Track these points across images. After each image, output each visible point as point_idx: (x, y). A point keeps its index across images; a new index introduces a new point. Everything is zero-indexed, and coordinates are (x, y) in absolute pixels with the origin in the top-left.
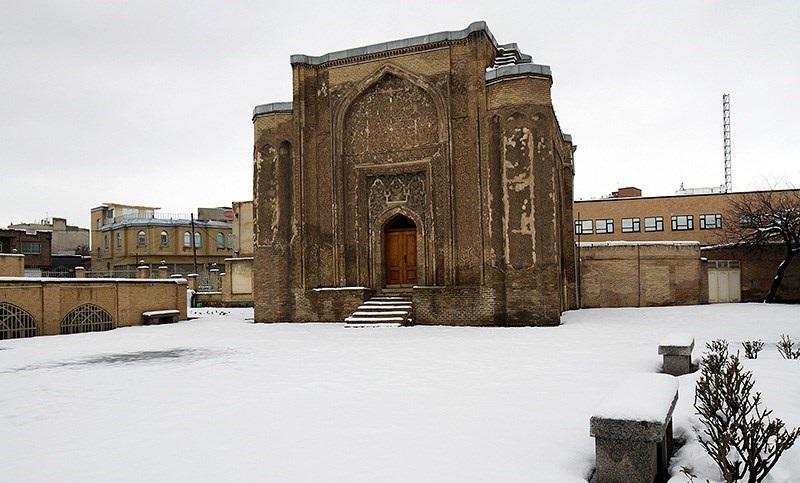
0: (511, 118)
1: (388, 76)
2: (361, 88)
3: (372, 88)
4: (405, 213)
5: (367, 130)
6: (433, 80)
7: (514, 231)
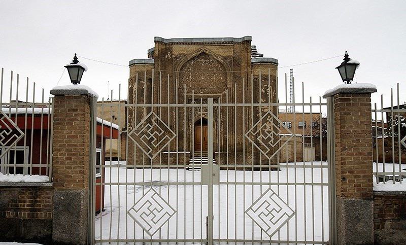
1: (203, 53)
2: (189, 57)
3: (193, 58)
6: (225, 58)
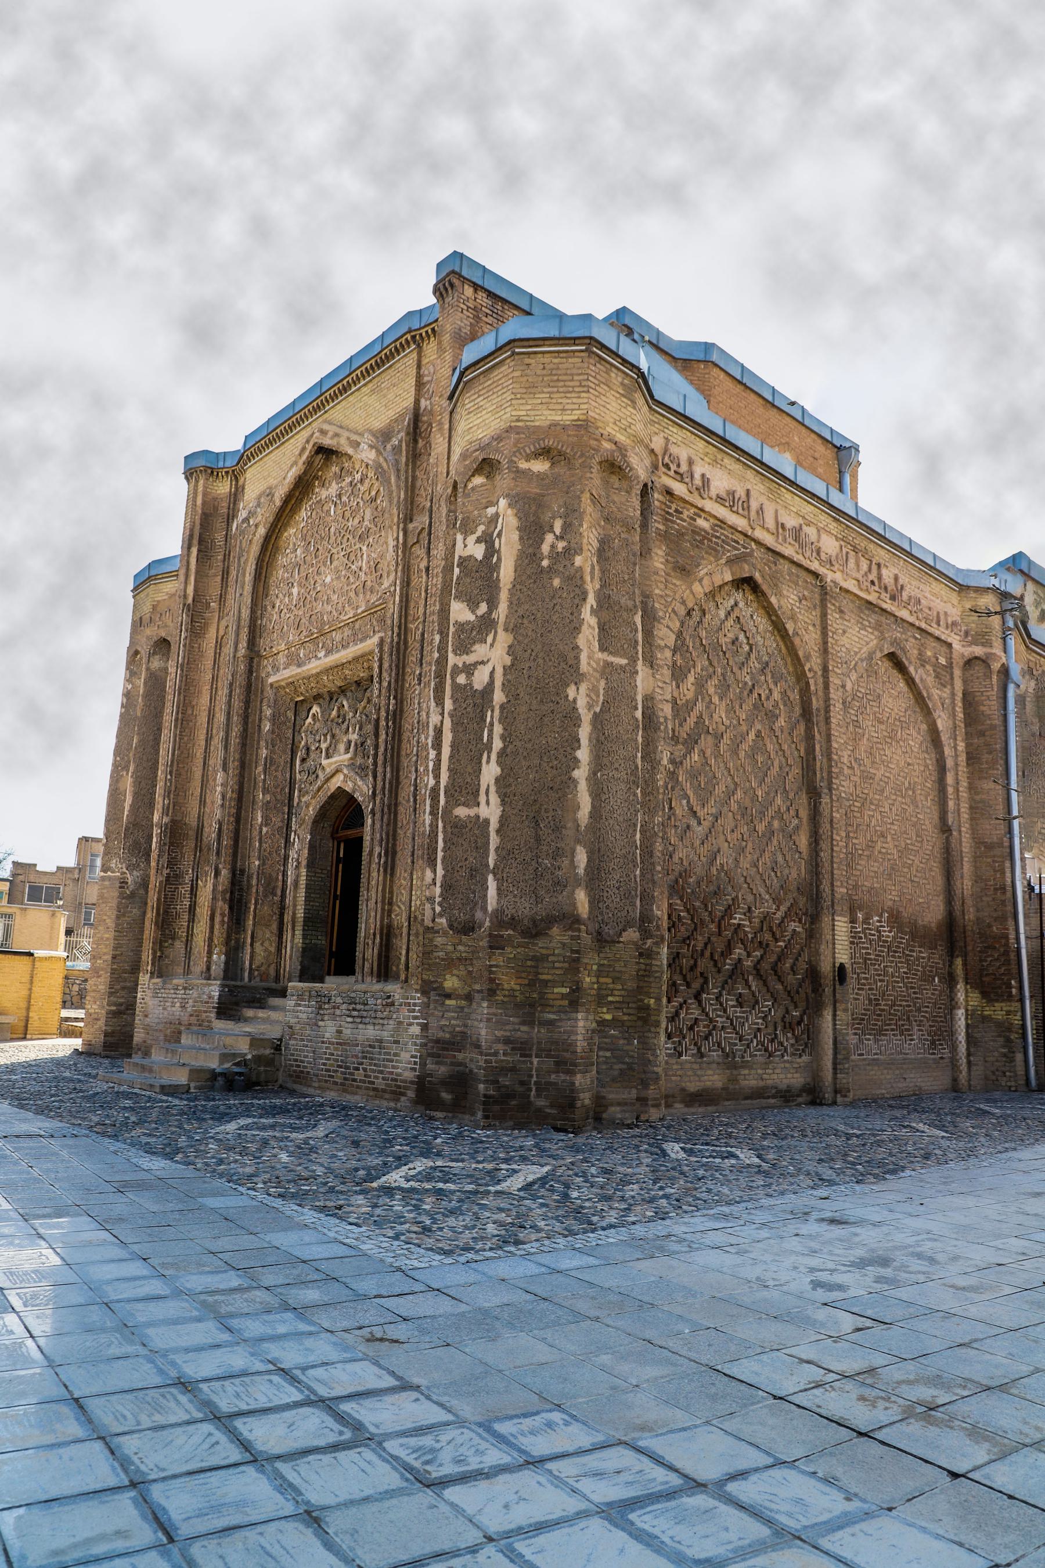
0: (478, 480)
2: (280, 493)
4: (349, 787)
5: (295, 591)
7: (461, 812)
